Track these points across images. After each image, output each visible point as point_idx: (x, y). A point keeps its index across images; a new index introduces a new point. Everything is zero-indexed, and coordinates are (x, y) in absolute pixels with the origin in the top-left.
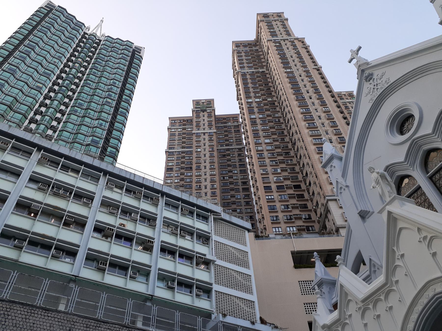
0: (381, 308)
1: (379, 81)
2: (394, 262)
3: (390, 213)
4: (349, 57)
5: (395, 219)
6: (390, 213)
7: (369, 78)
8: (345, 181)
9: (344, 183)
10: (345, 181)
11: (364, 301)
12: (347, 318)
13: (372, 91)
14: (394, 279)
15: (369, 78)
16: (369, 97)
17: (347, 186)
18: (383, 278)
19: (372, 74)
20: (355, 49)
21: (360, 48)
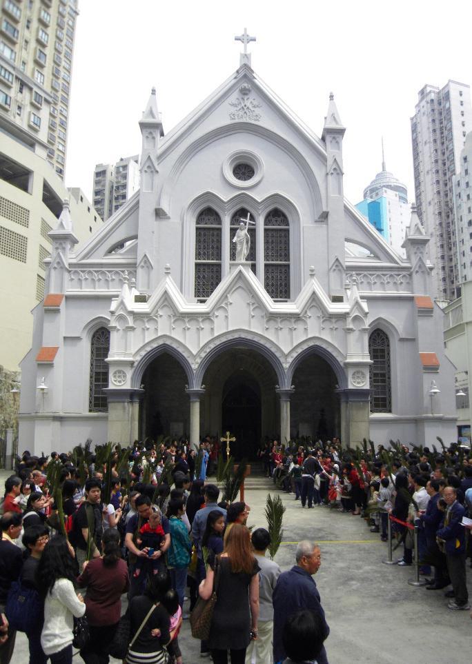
0: (192, 326)
1: (250, 107)
2: (222, 303)
3: (240, 271)
4: (239, 35)
5: (240, 277)
6: (240, 271)
7: (244, 92)
8: (158, 164)
9: (156, 164)
10: (158, 164)
11: (182, 314)
12: (157, 317)
13: (240, 107)
14: (216, 314)
15: (244, 92)
16: (233, 110)
17: (157, 172)
18: (206, 307)
19: (249, 91)
20: (252, 35)
21: (254, 40)
